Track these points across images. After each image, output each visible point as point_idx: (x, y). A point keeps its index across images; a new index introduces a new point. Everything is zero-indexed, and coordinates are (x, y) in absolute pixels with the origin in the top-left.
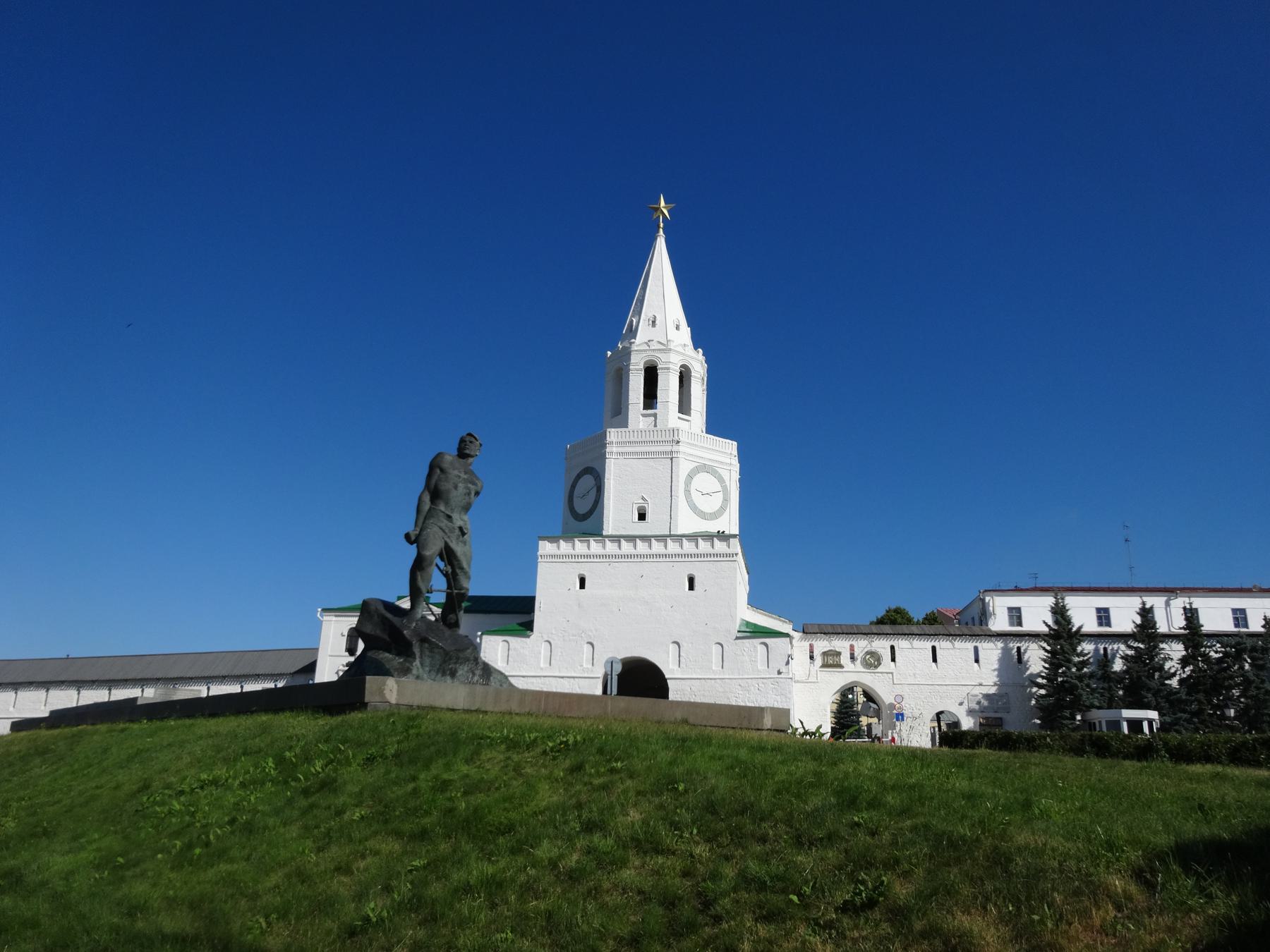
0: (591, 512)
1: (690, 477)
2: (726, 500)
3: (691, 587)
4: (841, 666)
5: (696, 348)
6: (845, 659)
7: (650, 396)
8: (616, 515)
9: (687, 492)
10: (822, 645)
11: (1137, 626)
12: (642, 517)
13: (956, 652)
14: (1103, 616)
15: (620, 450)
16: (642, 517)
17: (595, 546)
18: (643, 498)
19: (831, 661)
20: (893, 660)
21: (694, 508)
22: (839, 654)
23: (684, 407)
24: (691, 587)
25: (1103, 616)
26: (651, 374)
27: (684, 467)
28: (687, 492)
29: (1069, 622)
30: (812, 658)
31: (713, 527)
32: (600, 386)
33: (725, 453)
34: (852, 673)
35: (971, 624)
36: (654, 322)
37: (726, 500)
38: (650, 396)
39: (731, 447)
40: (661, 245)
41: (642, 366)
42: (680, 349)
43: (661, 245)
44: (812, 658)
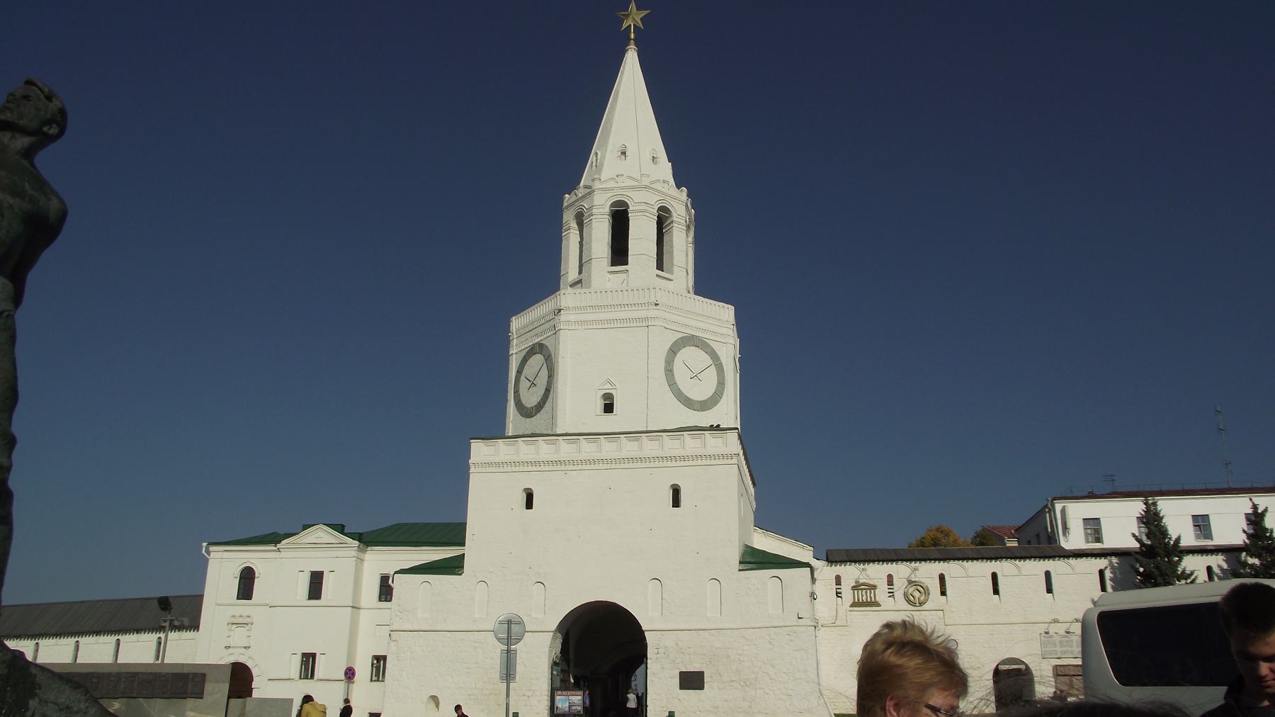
0: (540, 406)
2: (721, 384)
3: (676, 502)
4: (877, 604)
5: (678, 187)
6: (881, 594)
7: (619, 253)
10: (851, 573)
11: (1249, 536)
12: (609, 408)
13: (1023, 575)
14: (1202, 524)
15: (579, 317)
16: (609, 408)
17: (543, 449)
18: (610, 382)
19: (864, 599)
20: (943, 593)
22: (874, 587)
24: (676, 502)
25: (1202, 524)
26: (620, 219)
28: (669, 371)
29: (1164, 533)
30: (838, 594)
31: (705, 419)
33: (718, 321)
34: (893, 610)
35: (1039, 542)
36: (624, 153)
37: (721, 384)
38: (619, 253)
39: (726, 313)
41: (607, 209)
43: (631, 60)
44: (838, 594)
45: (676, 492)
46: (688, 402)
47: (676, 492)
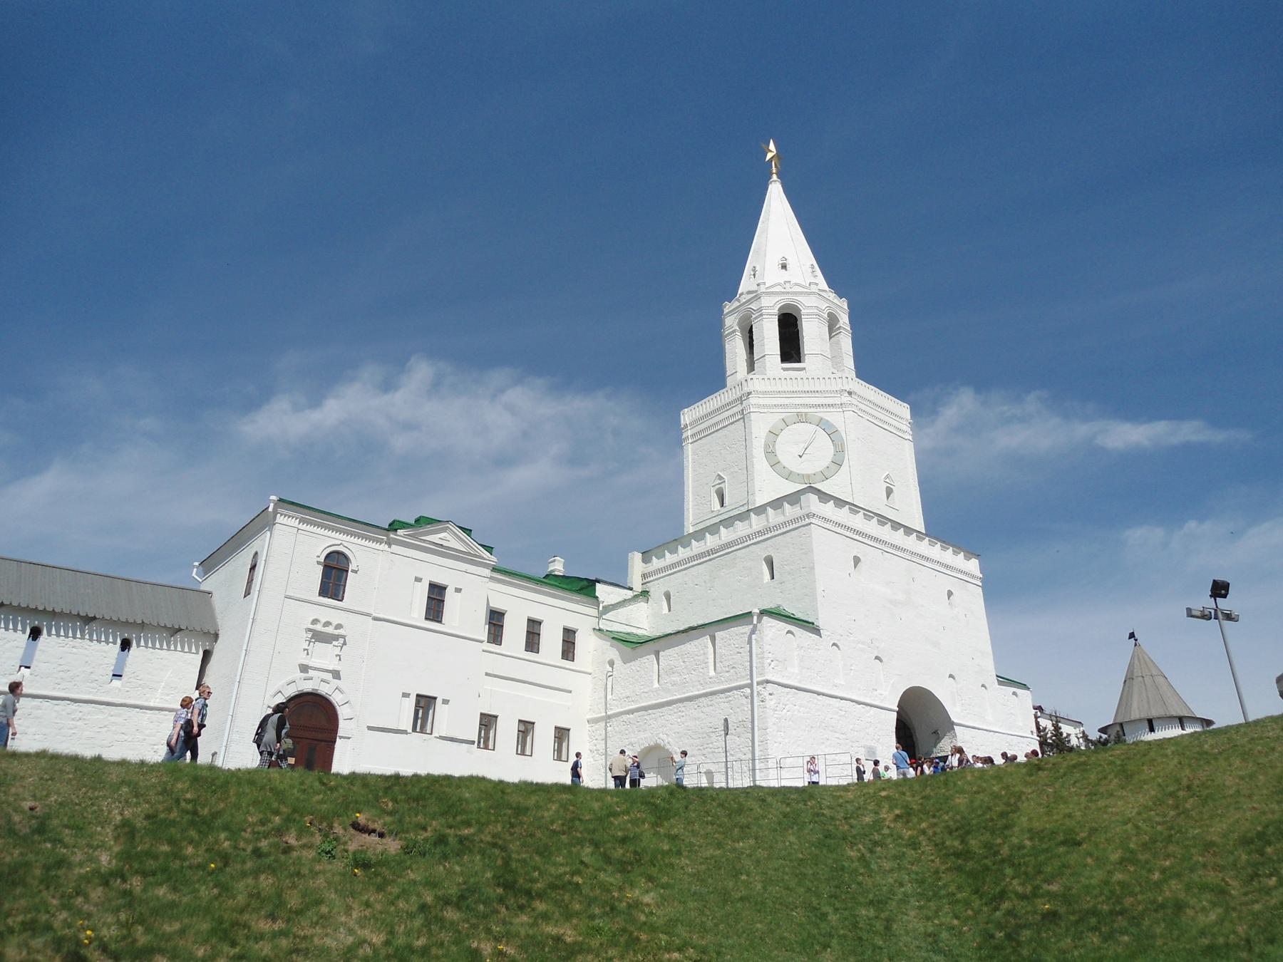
9: (770, 452)
18: (720, 477)
27: (760, 426)
28: (770, 452)
45: (770, 563)
47: (770, 563)
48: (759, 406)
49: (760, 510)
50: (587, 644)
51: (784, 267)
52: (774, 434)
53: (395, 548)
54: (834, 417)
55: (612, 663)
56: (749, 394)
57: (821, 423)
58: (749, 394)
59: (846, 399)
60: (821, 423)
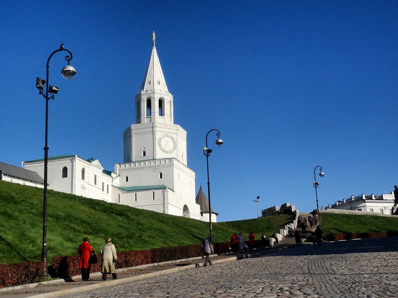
1: (160, 139)
3: (161, 177)
8: (135, 154)
12: (144, 155)
16: (144, 155)
21: (163, 150)
23: (162, 113)
26: (149, 102)
27: (158, 136)
28: (160, 145)
32: (135, 107)
36: (150, 83)
40: (154, 51)
41: (146, 100)
42: (159, 92)
43: (154, 51)
45: (161, 174)
46: (166, 152)
48: (159, 131)
49: (160, 160)
50: (110, 188)
51: (159, 83)
52: (160, 139)
53: (91, 167)
54: (174, 136)
55: (119, 195)
56: (155, 127)
57: (172, 138)
58: (155, 127)
59: (177, 132)
60: (172, 138)
